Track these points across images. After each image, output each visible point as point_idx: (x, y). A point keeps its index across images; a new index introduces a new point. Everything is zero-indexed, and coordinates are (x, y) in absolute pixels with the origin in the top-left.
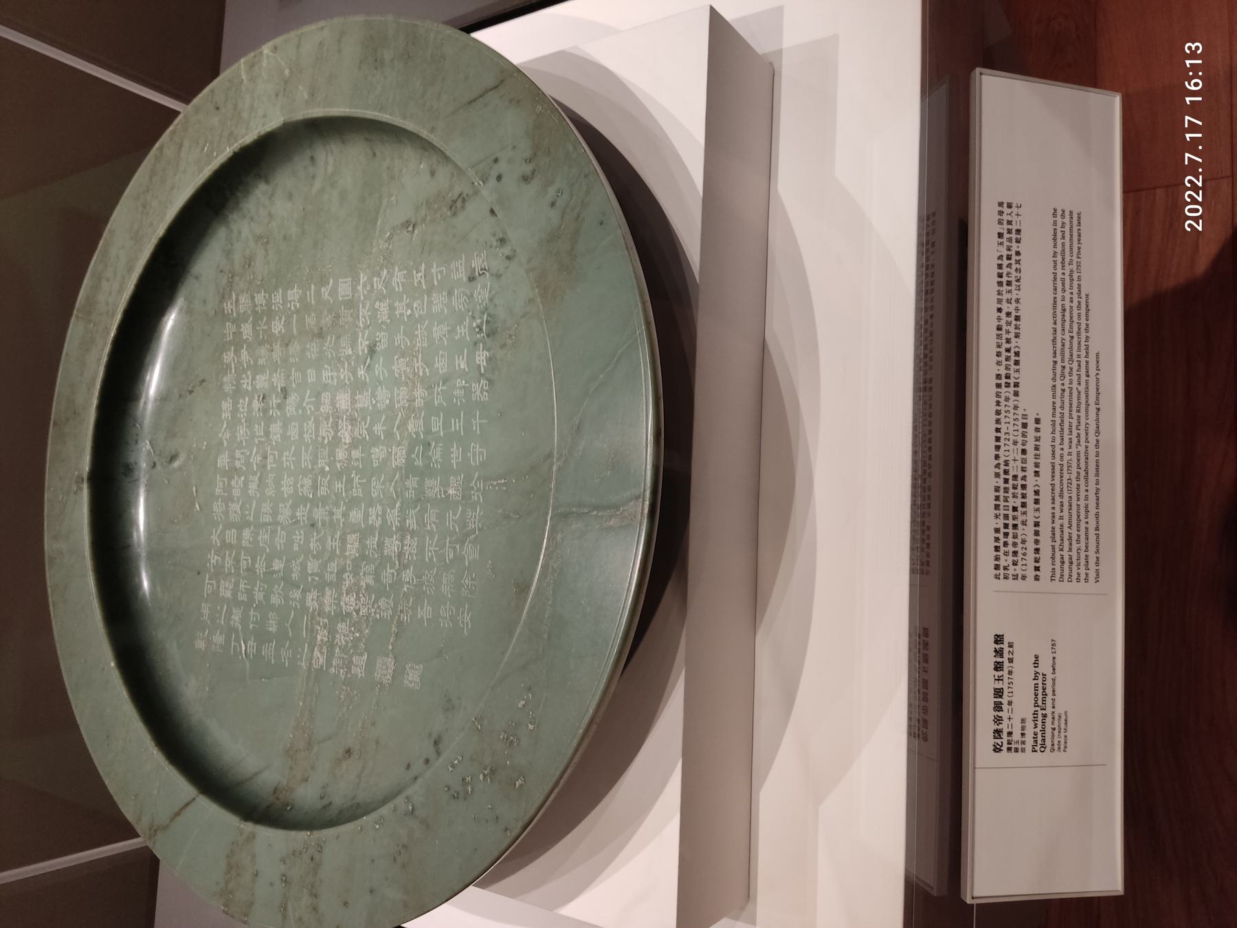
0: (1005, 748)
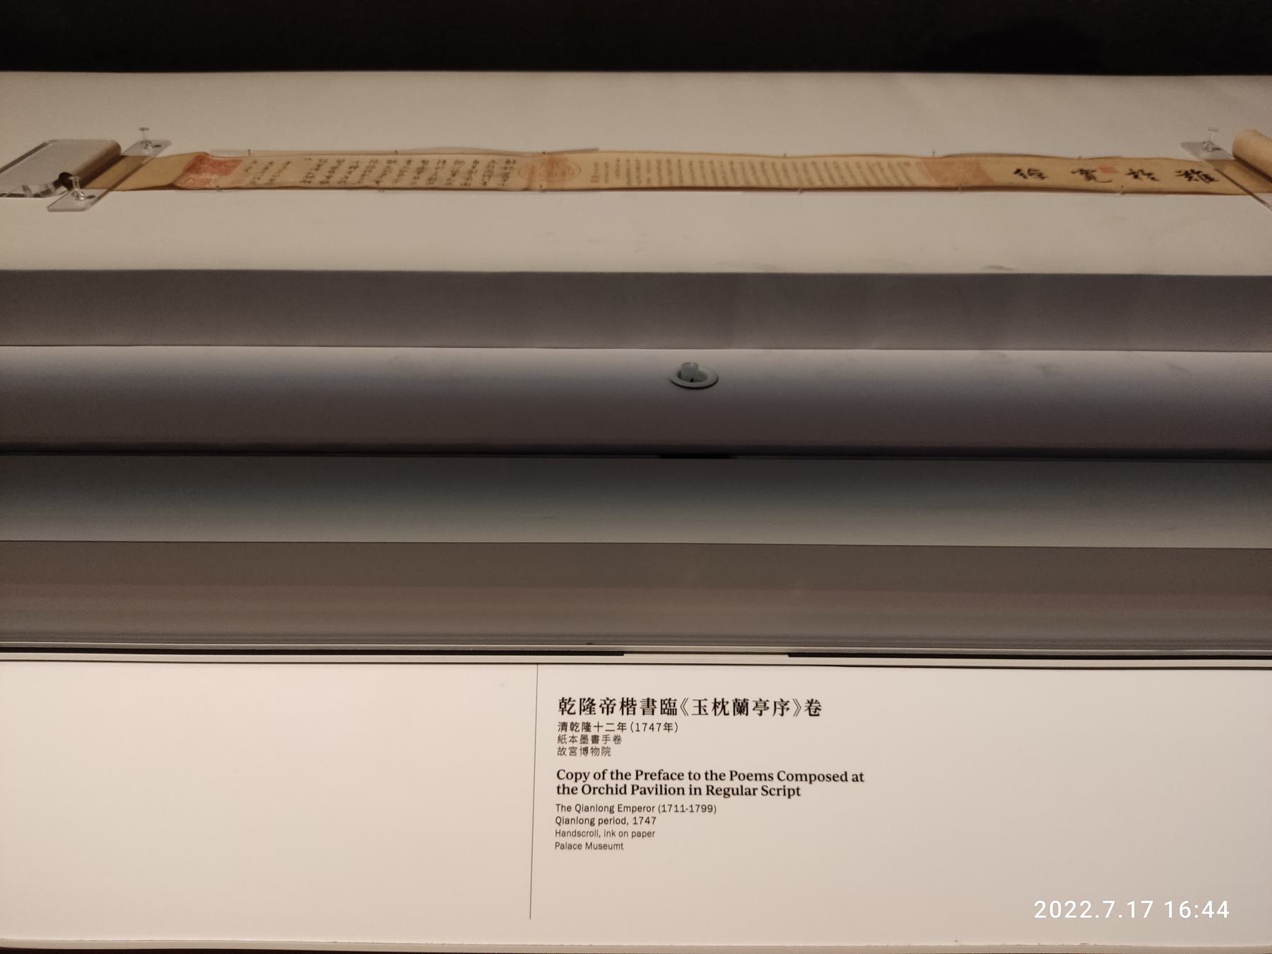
0: (568, 719)
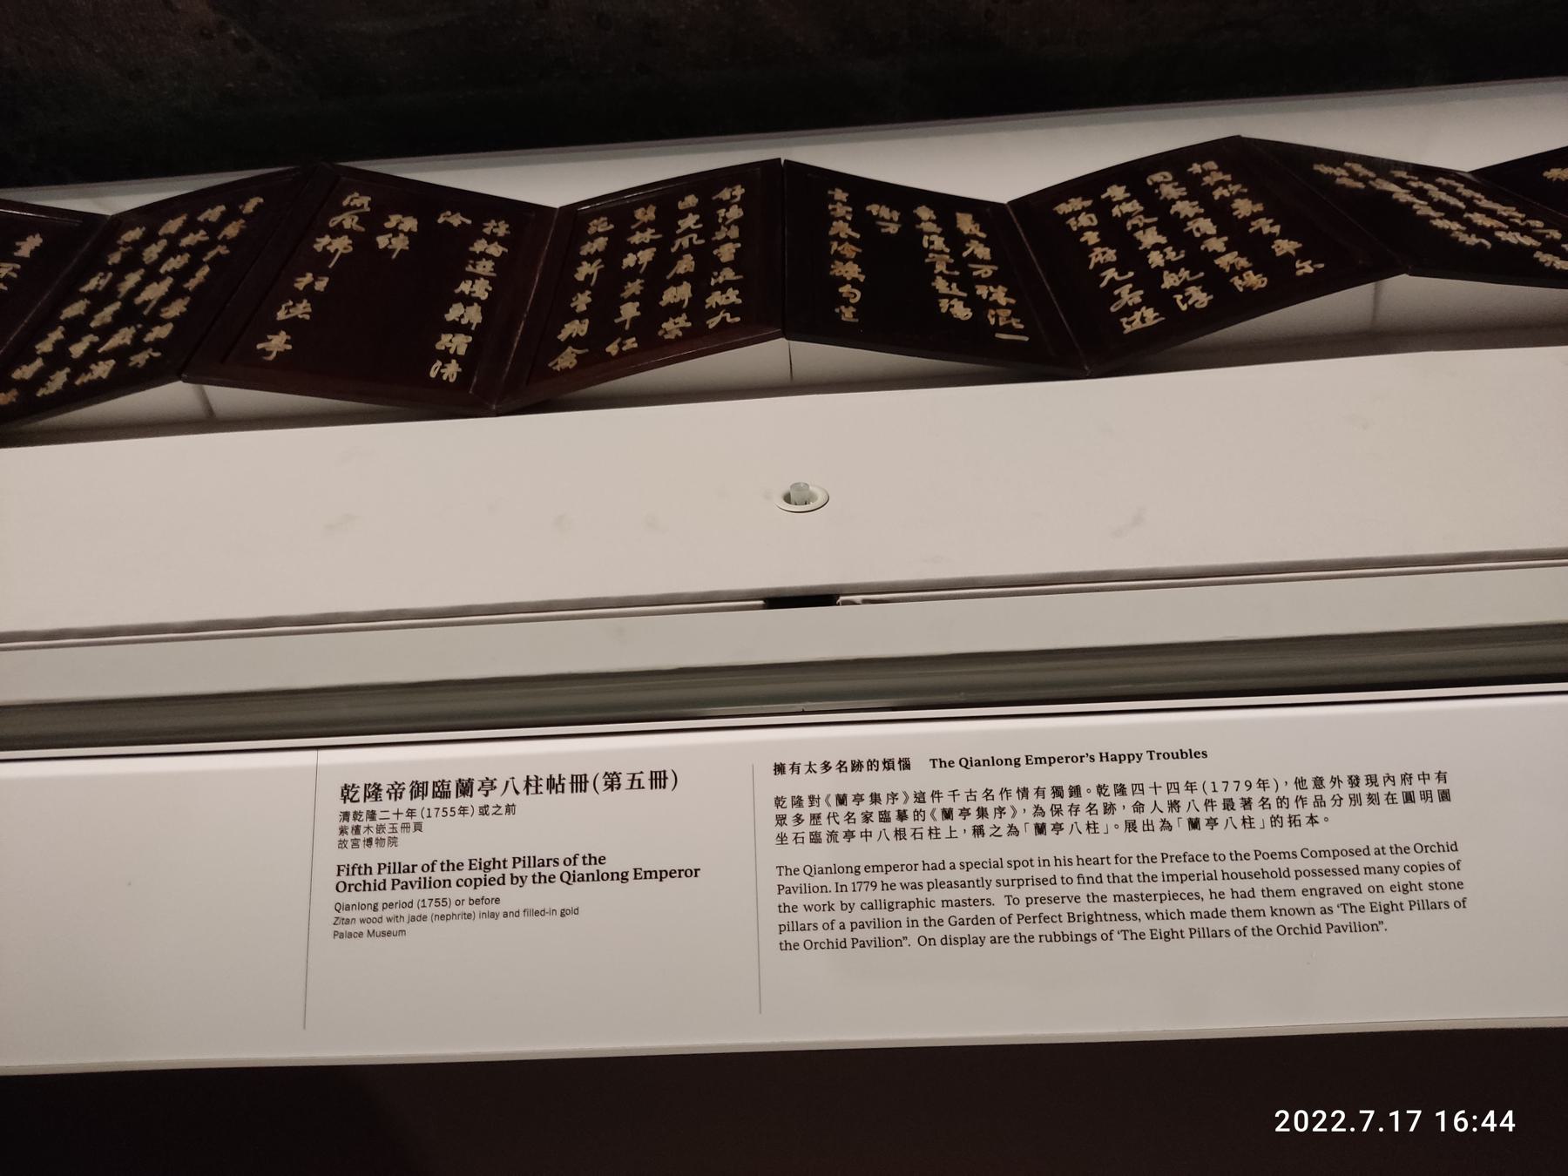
0: (350, 807)
